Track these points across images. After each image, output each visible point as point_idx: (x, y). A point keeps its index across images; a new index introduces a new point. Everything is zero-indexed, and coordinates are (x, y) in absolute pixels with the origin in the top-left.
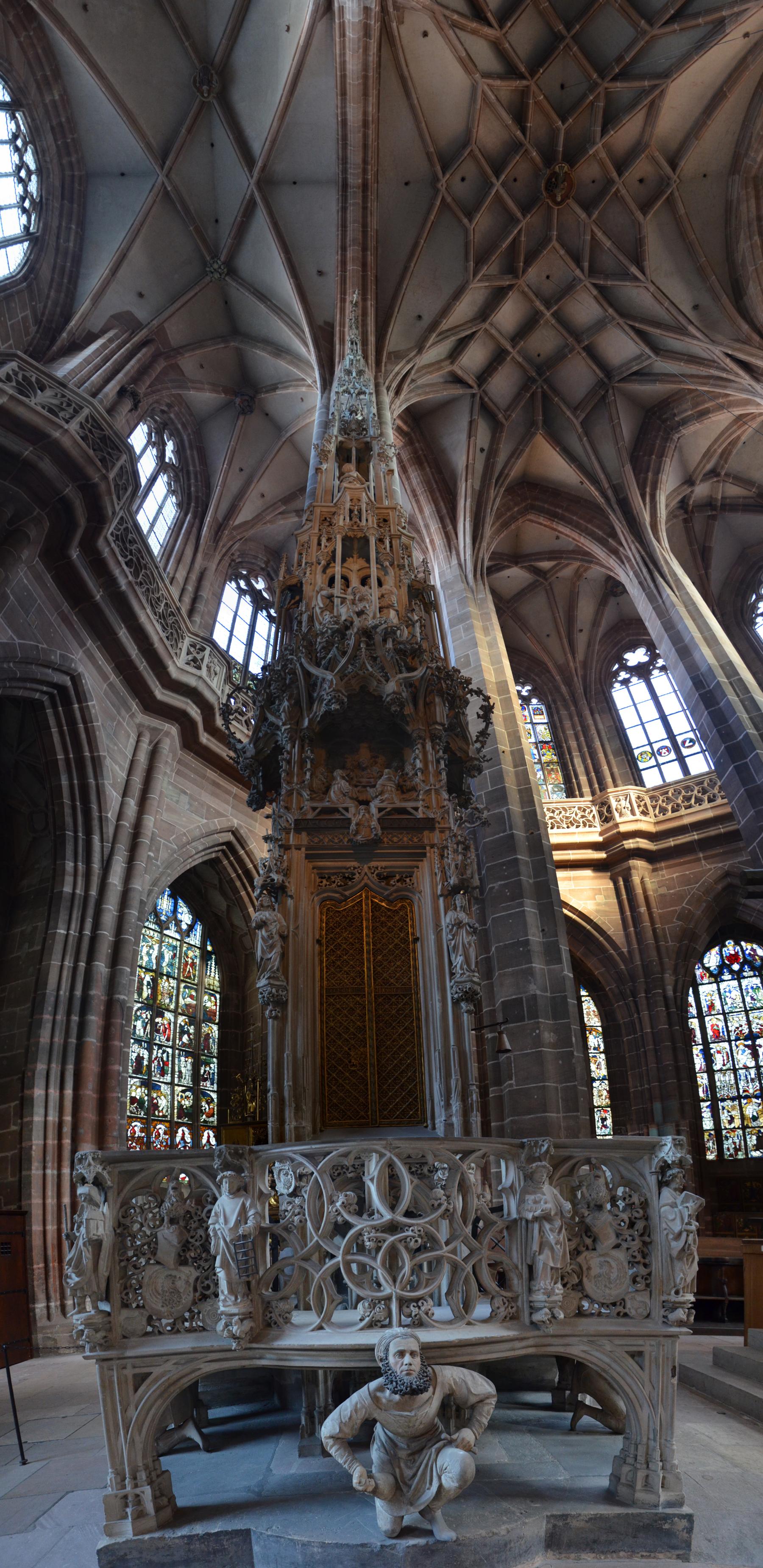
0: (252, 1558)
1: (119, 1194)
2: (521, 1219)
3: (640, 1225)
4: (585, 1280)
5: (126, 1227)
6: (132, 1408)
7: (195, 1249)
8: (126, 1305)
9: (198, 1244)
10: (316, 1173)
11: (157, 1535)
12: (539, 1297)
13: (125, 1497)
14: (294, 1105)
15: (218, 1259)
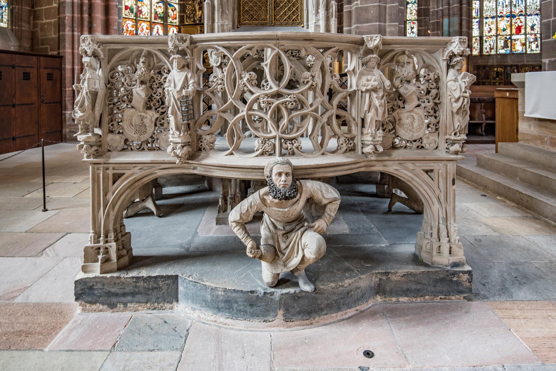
0: (177, 294)
2: (358, 90)
3: (434, 92)
4: (397, 126)
5: (113, 84)
6: (110, 194)
7: (156, 102)
8: (111, 132)
10: (231, 60)
11: (115, 275)
13: (99, 248)
14: (221, 10)
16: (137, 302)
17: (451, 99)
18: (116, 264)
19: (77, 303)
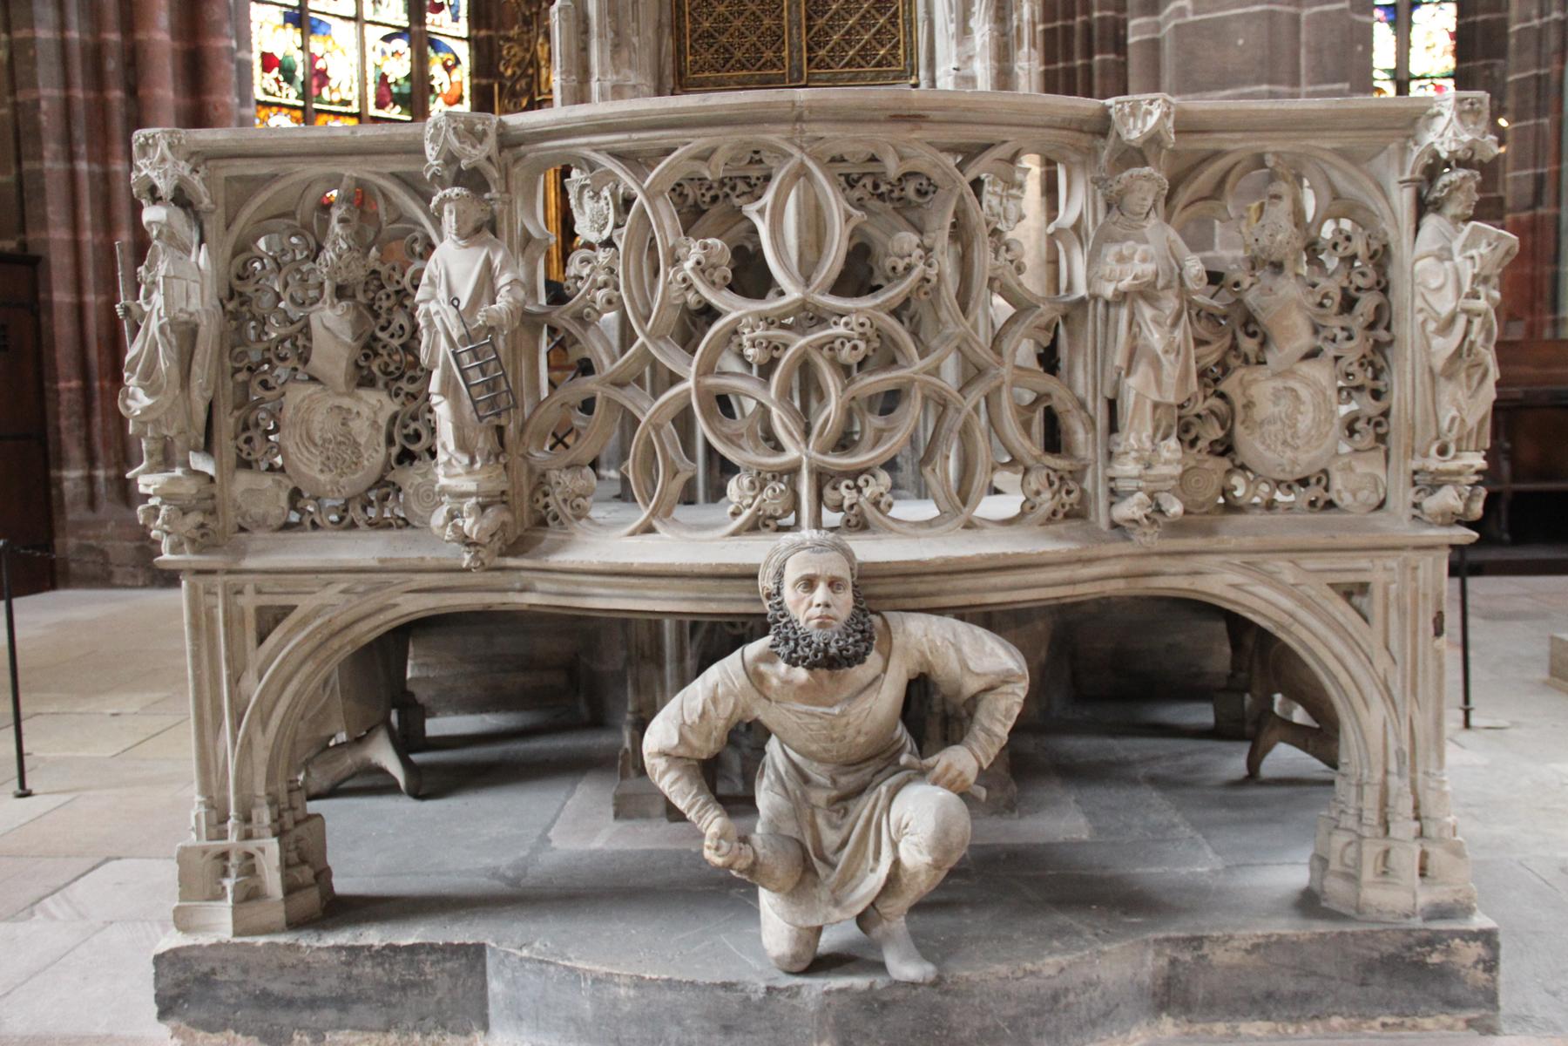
1: (228, 227)
5: (245, 301)
7: (386, 358)
8: (245, 464)
9: (396, 343)
12: (1128, 468)
15: (436, 376)
16: (354, 1028)
17: (1424, 323)
18: (282, 907)
19: (164, 1030)
